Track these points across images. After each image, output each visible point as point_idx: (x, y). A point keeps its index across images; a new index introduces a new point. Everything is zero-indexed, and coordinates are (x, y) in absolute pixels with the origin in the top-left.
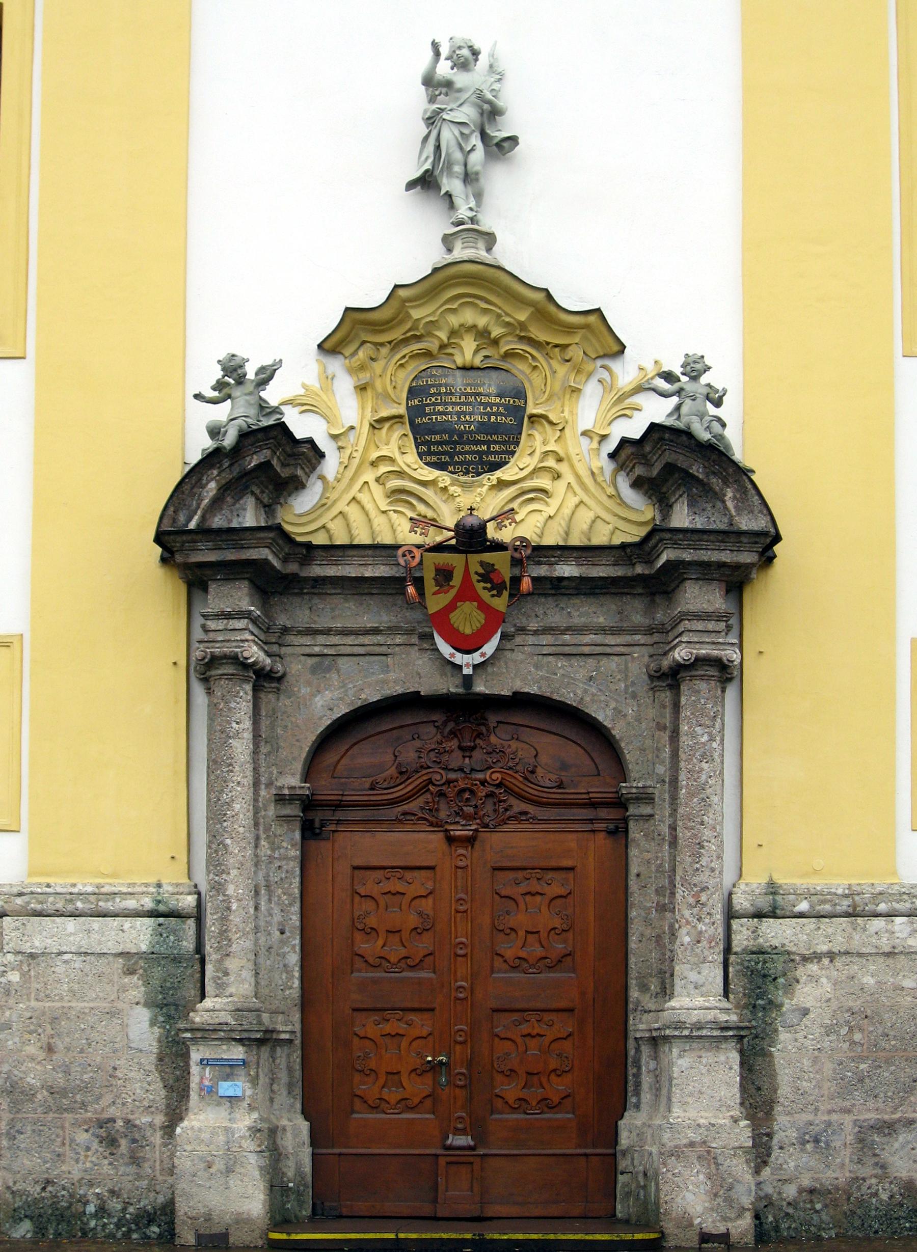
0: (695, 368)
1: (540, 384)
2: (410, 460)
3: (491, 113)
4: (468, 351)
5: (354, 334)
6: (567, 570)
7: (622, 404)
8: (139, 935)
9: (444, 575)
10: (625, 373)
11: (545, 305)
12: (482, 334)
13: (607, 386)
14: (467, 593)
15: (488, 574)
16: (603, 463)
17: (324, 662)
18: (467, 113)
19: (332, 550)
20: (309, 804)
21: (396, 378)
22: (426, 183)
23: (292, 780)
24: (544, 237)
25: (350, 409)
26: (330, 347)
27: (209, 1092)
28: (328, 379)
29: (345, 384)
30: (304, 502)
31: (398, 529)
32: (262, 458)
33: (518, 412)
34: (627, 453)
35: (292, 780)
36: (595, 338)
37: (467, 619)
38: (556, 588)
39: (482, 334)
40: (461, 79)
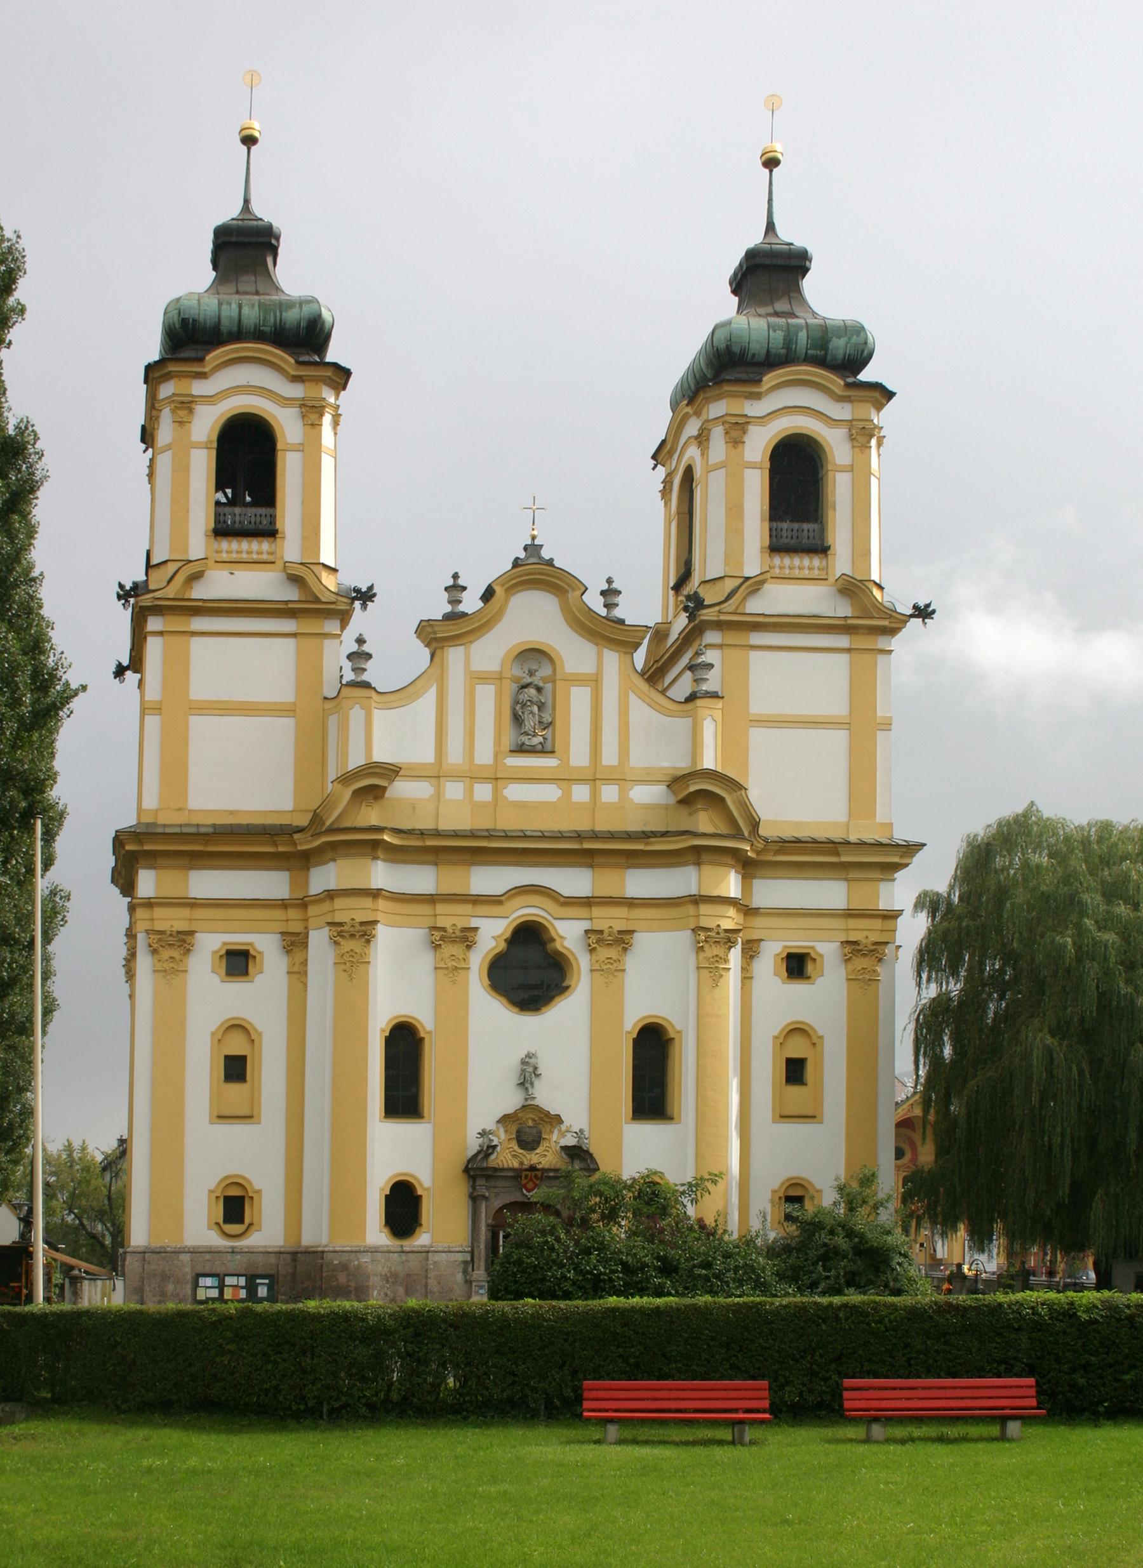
0: (581, 1131)
1: (545, 1129)
2: (516, 1148)
3: (536, 1068)
4: (530, 1123)
5: (504, 1120)
6: (552, 1174)
7: (562, 1135)
8: (460, 1257)
9: (526, 1176)
10: (563, 1127)
11: (547, 1114)
12: (533, 1120)
13: (560, 1131)
14: (531, 1180)
15: (536, 1176)
16: (558, 1148)
17: (497, 1195)
18: (531, 1069)
19: (503, 1170)
20: (493, 1226)
21: (514, 1128)
22: (522, 1084)
23: (490, 1221)
24: (546, 1097)
25: (503, 1135)
26: (498, 1122)
27: (477, 1293)
28: (498, 1129)
29: (502, 1130)
30: (493, 1157)
31: (516, 1165)
32: (488, 1150)
33: (540, 1137)
34: (565, 1148)
35: (490, 1221)
36: (558, 1120)
37: (530, 1185)
38: (549, 1178)
39: (533, 1120)
40: (531, 1061)
